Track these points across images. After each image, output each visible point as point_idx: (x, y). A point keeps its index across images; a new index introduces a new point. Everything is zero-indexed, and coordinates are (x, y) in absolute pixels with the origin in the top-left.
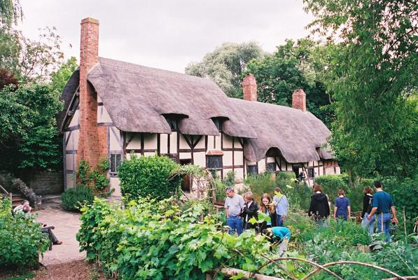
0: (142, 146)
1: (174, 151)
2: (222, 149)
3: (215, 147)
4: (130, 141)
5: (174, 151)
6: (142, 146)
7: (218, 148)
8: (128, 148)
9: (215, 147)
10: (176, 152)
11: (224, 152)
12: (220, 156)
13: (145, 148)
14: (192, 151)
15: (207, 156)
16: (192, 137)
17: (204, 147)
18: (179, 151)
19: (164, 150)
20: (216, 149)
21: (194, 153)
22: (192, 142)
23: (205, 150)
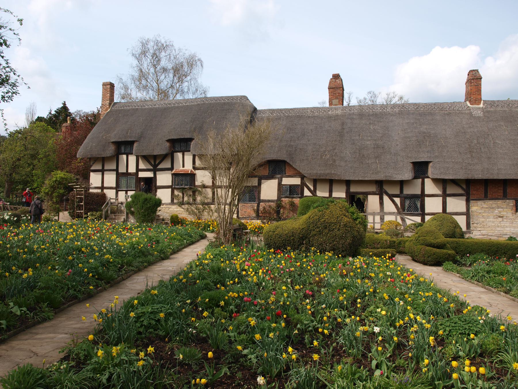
0: (103, 166)
1: (132, 169)
2: (194, 168)
3: (183, 166)
4: (93, 164)
5: (132, 169)
6: (103, 166)
7: (188, 167)
8: (92, 168)
9: (183, 166)
10: (135, 171)
11: (197, 172)
12: (192, 176)
13: (106, 168)
14: (155, 170)
15: (172, 174)
16: (155, 157)
17: (169, 166)
18: (138, 170)
19: (122, 170)
20: (185, 168)
21: (157, 173)
22: (155, 162)
23: (172, 169)
